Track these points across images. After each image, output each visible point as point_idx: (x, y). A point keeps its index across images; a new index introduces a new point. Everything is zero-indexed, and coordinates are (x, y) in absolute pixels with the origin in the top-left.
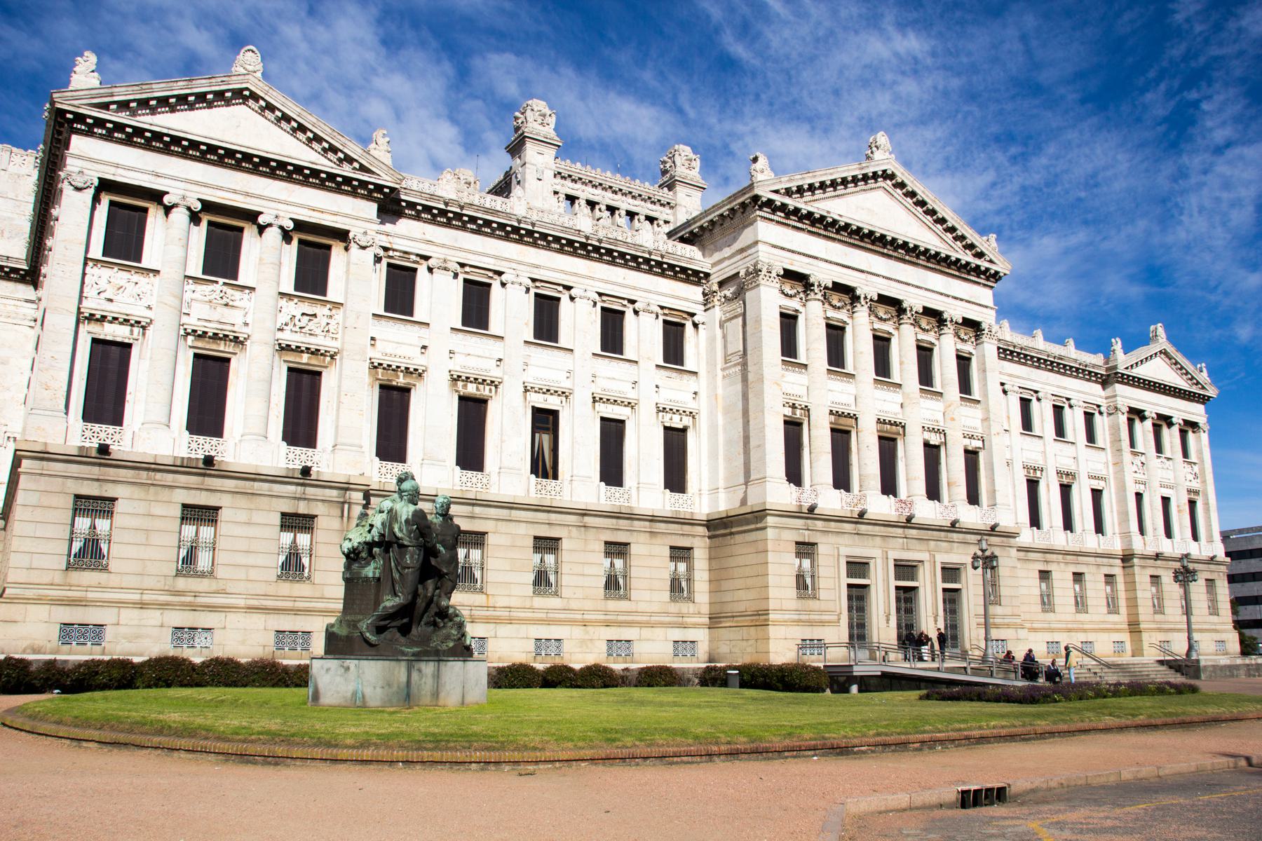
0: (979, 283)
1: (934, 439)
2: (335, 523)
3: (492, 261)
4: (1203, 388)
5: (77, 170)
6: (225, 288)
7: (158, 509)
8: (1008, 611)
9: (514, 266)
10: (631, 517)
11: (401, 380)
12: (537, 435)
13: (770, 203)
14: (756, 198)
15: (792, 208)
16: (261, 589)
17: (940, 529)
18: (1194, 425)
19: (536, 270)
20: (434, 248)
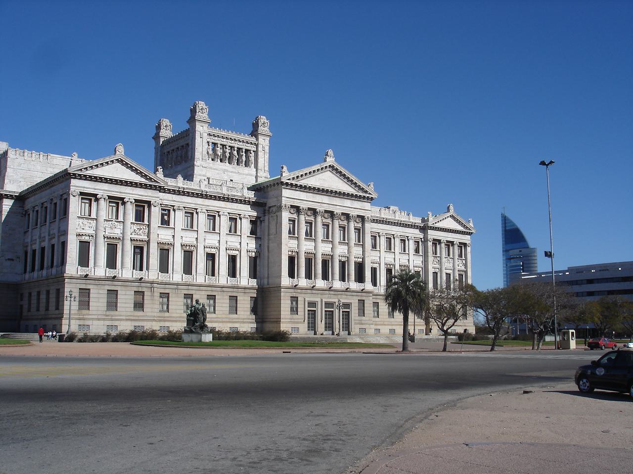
0: (365, 202)
1: (343, 259)
2: (149, 294)
3: (194, 205)
4: (470, 229)
5: (73, 190)
6: (115, 223)
7: (101, 292)
8: (367, 319)
9: (201, 206)
10: (238, 288)
11: (166, 247)
12: (208, 262)
13: (287, 184)
14: (282, 182)
15: (294, 184)
16: (129, 314)
17: (342, 291)
18: (465, 245)
19: (208, 207)
20: (176, 203)
